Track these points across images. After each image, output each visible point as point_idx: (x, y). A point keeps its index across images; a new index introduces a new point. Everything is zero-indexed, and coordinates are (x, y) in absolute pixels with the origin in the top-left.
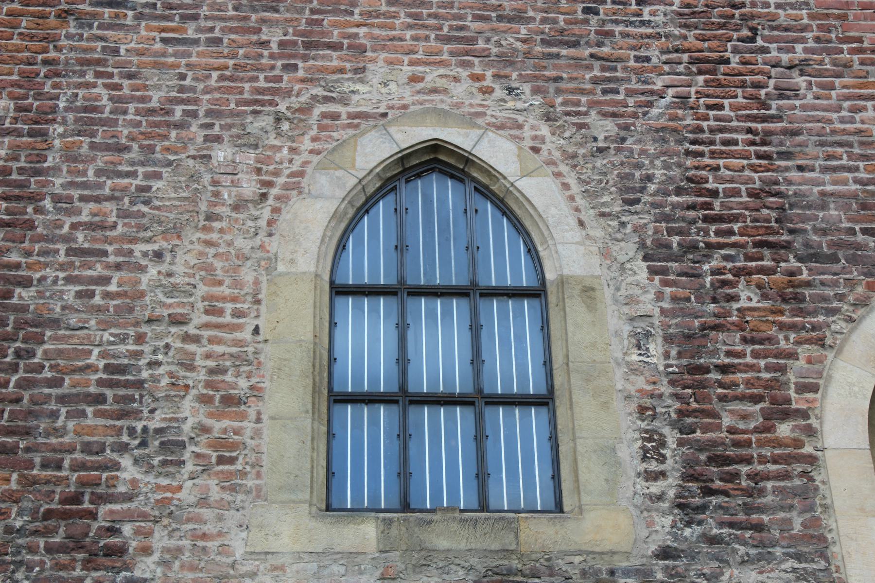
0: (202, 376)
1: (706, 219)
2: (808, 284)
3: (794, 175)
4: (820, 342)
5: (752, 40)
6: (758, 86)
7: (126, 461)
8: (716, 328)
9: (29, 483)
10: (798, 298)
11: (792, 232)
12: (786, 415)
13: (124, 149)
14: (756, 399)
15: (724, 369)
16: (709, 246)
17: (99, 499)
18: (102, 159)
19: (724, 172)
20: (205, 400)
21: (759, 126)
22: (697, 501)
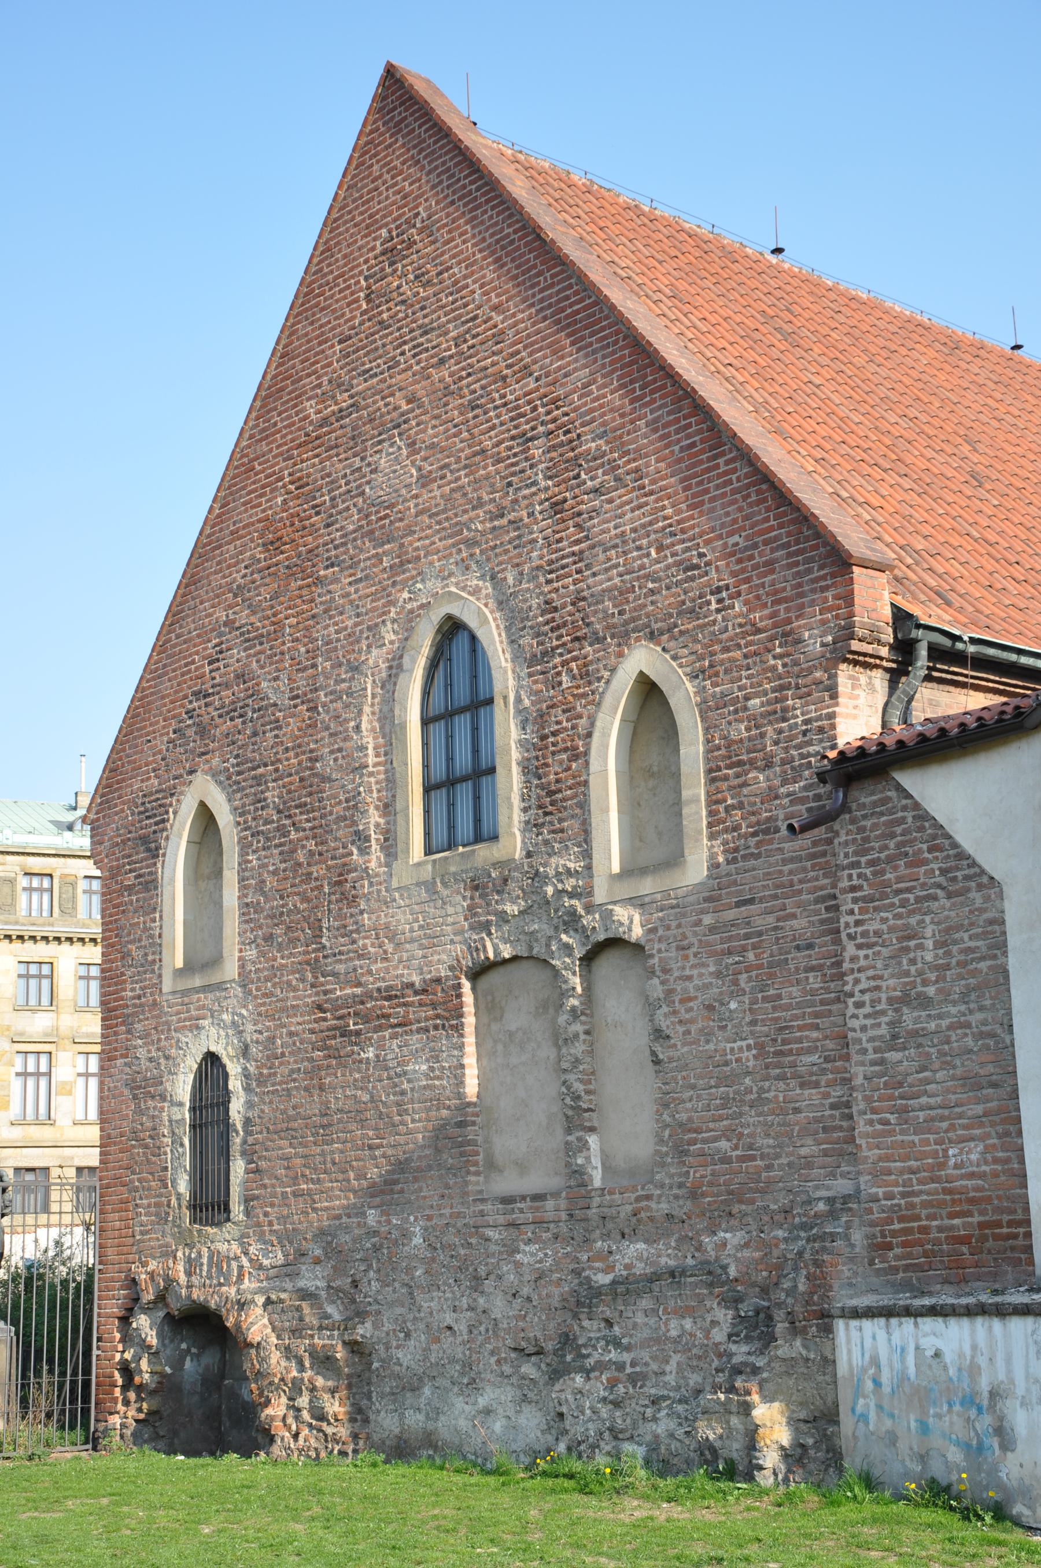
0: (375, 795)
1: (552, 630)
2: (591, 662)
3: (590, 581)
4: (592, 703)
5: (577, 476)
6: (579, 514)
7: (355, 851)
8: (552, 707)
9: (328, 868)
10: (587, 674)
11: (588, 625)
12: (575, 757)
13: (340, 665)
14: (566, 749)
15: (554, 734)
16: (553, 649)
17: (349, 872)
18: (336, 672)
19: (561, 590)
20: (377, 808)
21: (576, 548)
22: (541, 821)
